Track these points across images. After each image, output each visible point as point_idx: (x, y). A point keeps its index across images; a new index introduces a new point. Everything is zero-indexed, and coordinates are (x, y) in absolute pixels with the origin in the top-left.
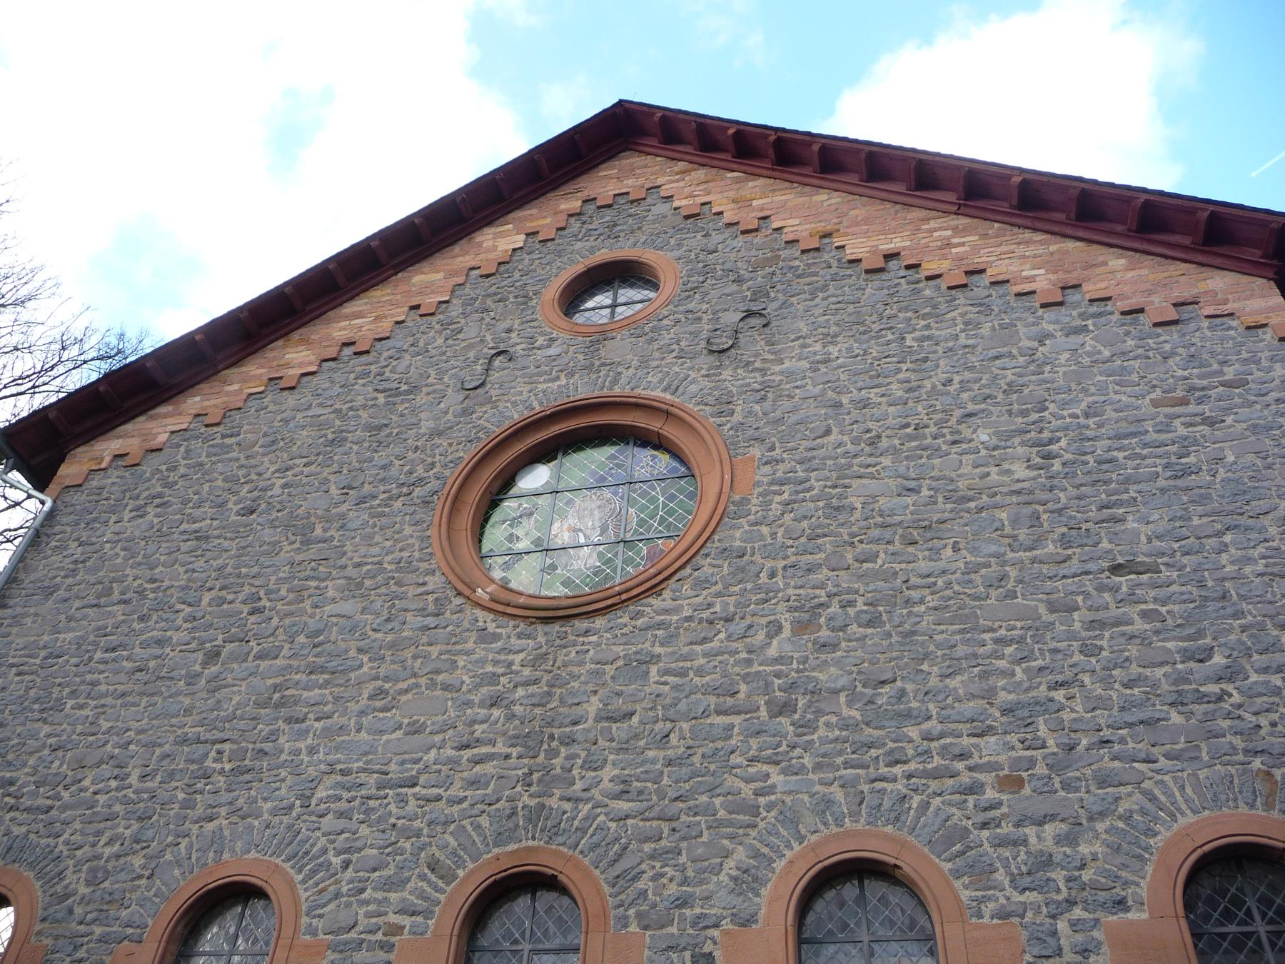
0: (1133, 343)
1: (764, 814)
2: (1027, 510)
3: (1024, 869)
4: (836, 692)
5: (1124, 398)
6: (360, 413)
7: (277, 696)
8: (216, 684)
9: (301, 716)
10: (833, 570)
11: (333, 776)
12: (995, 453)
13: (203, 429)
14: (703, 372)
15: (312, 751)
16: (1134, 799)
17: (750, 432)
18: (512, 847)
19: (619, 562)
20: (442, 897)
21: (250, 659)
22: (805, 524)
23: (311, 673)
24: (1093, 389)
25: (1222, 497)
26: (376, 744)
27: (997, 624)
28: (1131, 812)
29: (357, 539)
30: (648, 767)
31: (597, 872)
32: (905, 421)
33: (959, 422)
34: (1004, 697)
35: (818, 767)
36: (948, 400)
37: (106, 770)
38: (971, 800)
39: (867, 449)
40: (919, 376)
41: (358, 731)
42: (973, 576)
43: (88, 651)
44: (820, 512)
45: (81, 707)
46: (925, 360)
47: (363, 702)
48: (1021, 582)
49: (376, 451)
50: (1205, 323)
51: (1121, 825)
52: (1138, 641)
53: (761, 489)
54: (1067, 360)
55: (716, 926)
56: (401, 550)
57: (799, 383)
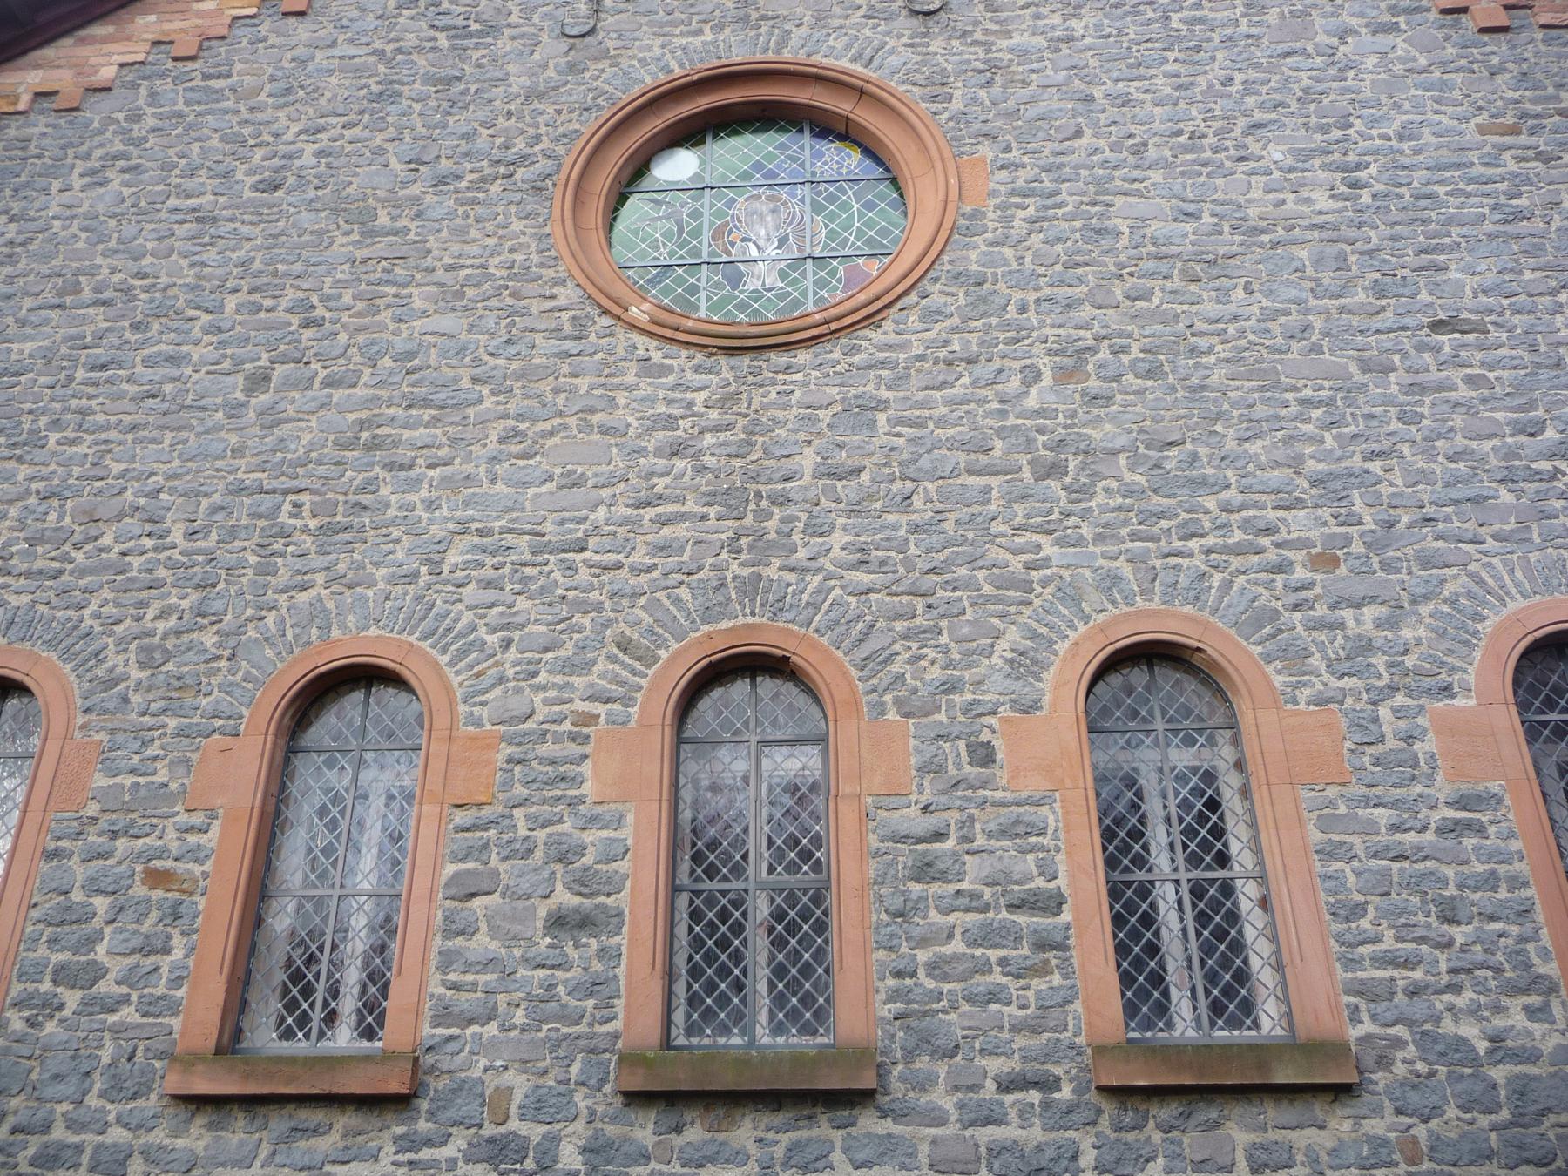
0: (1454, 51)
1: (1039, 590)
2: (1332, 250)
3: (1342, 654)
4: (1115, 453)
5: (1445, 120)
6: (415, 57)
7: (365, 435)
8: (271, 419)
9: (407, 461)
10: (1099, 308)
11: (467, 537)
12: (1291, 176)
13: (170, 64)
14: (905, 40)
15: (431, 505)
16: (1459, 581)
17: (977, 126)
18: (725, 624)
19: (809, 283)
20: (644, 682)
21: (316, 386)
22: (1059, 248)
23: (410, 407)
24: (1407, 106)
25: (1557, 248)
26: (521, 498)
27: (1301, 383)
28: (1457, 594)
29: (444, 233)
30: (888, 533)
31: (839, 653)
32: (1177, 127)
33: (1245, 134)
34: (1311, 466)
35: (1099, 538)
36: (1228, 104)
37: (132, 524)
38: (1280, 579)
39: (1131, 159)
40: (1191, 70)
41: (493, 481)
42: (1270, 325)
43: (63, 368)
44: (1078, 235)
45: (73, 442)
46: (1198, 49)
47: (491, 446)
48: (1328, 334)
49: (449, 113)
50: (1539, 35)
51: (1446, 608)
52: (1464, 410)
53: (998, 201)
54: (1375, 65)
55: (993, 713)
56: (511, 251)
57: (1035, 66)
